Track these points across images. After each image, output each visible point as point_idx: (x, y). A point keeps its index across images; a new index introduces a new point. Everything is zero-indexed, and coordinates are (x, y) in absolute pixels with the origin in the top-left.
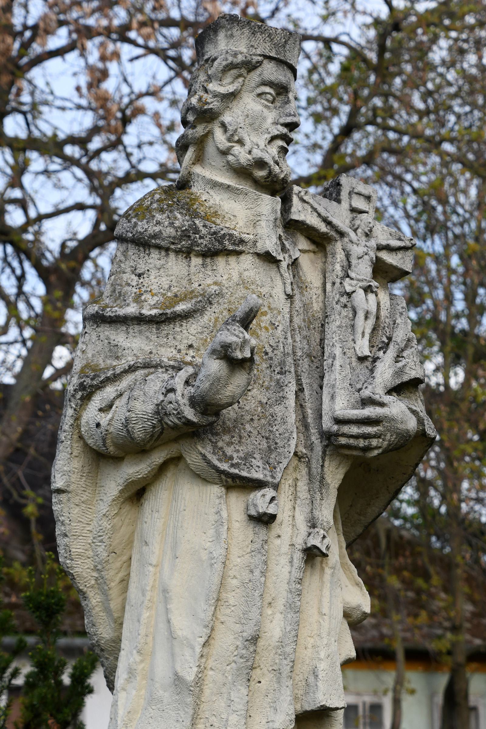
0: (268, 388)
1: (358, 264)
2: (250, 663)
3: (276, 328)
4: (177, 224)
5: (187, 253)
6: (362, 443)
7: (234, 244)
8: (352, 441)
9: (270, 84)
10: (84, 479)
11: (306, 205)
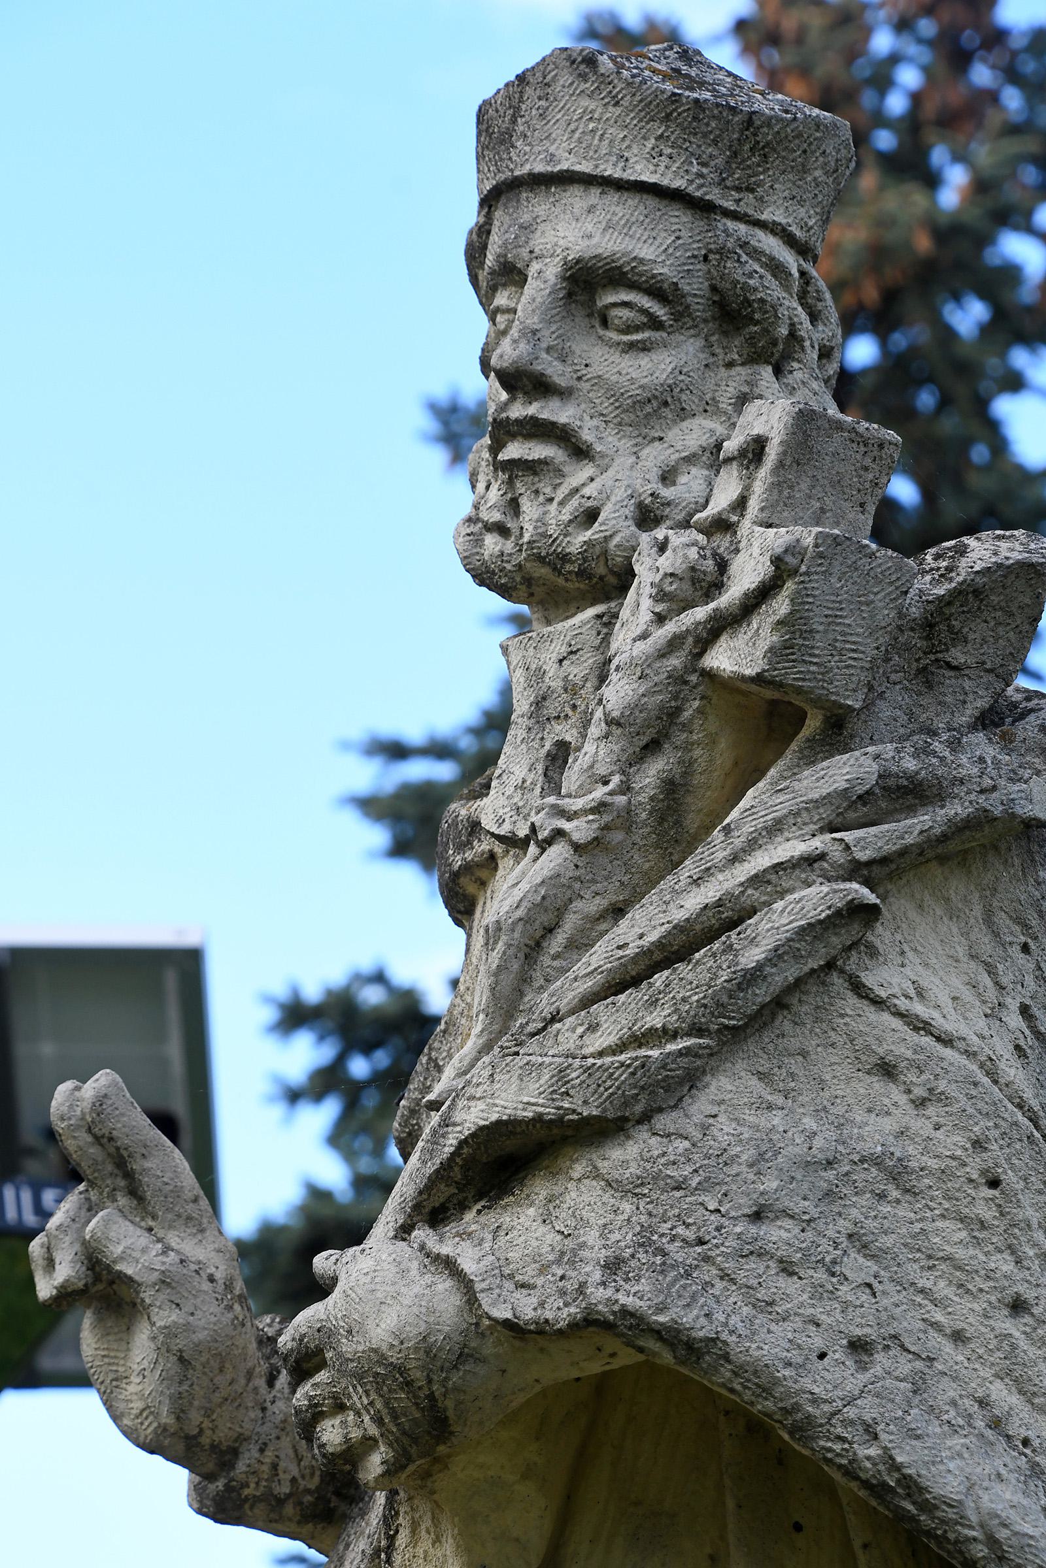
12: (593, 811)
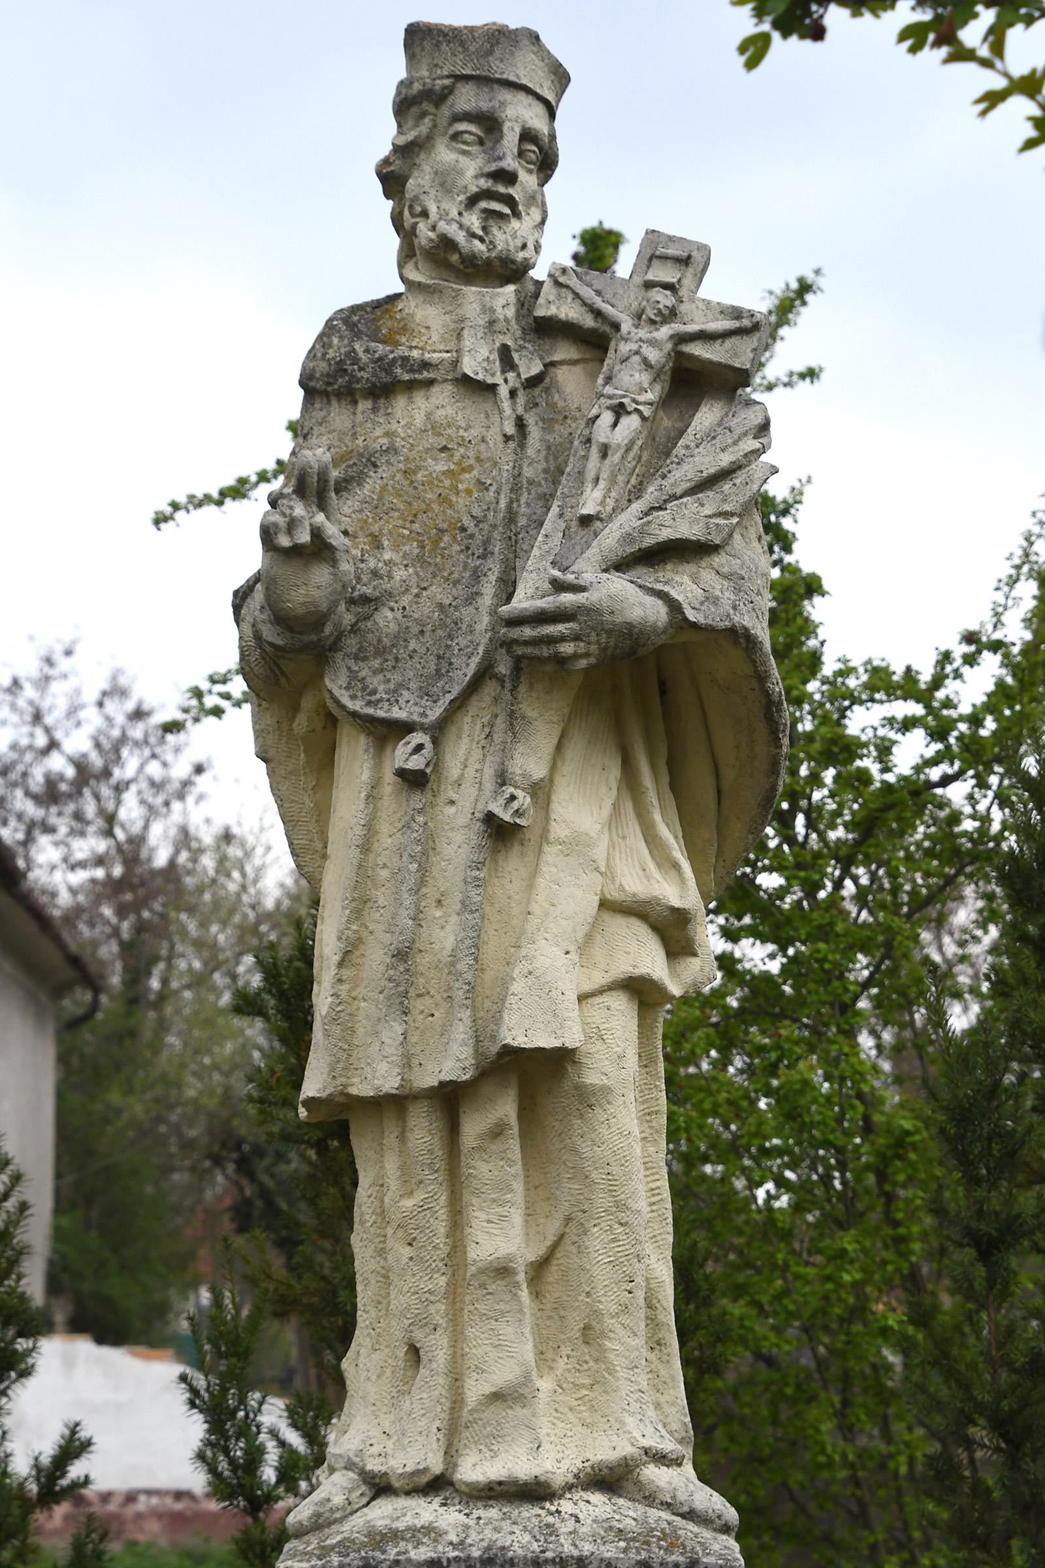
0: (456, 583)
1: (619, 371)
2: (401, 989)
3: (487, 489)
4: (331, 353)
5: (349, 395)
6: (545, 652)
7: (412, 371)
8: (529, 650)
9: (467, 117)
10: (285, 739)
11: (564, 290)
12: (651, 404)
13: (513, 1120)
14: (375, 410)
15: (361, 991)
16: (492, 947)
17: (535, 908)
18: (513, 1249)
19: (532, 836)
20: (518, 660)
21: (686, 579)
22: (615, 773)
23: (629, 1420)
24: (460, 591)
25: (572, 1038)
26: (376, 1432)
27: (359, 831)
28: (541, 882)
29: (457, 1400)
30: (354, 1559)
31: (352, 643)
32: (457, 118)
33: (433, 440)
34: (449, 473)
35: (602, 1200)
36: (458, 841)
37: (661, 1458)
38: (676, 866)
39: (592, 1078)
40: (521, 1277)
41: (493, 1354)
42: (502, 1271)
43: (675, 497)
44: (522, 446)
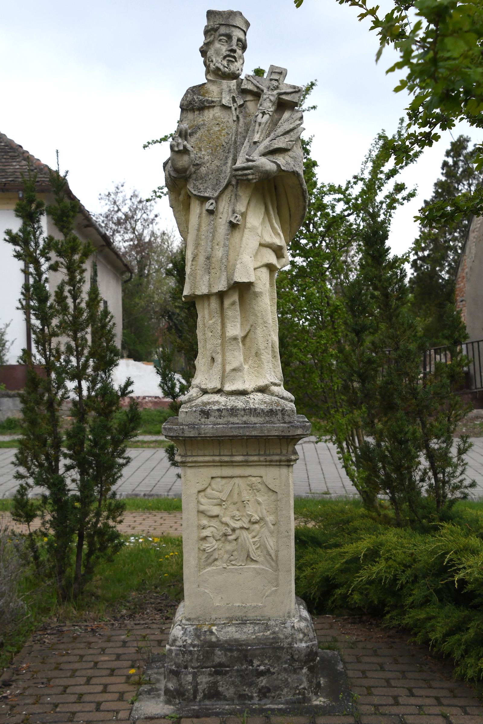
5: (193, 110)
6: (245, 178)
8: (240, 178)
13: (237, 300)
14: (199, 114)
15: (198, 268)
16: (232, 256)
17: (242, 246)
18: (237, 333)
19: (242, 227)
20: (238, 180)
21: (281, 158)
22: (263, 210)
23: (267, 375)
24: (222, 162)
25: (252, 279)
26: (204, 379)
27: (197, 226)
28: (244, 239)
29: (224, 371)
30: (199, 409)
31: (194, 176)
32: (220, 35)
33: (215, 122)
34: (219, 131)
35: (260, 321)
36: (222, 228)
37: (275, 384)
38: (279, 234)
39: (257, 290)
40: (240, 340)
41: (233, 359)
42: (235, 339)
43: (278, 136)
44: (238, 123)
